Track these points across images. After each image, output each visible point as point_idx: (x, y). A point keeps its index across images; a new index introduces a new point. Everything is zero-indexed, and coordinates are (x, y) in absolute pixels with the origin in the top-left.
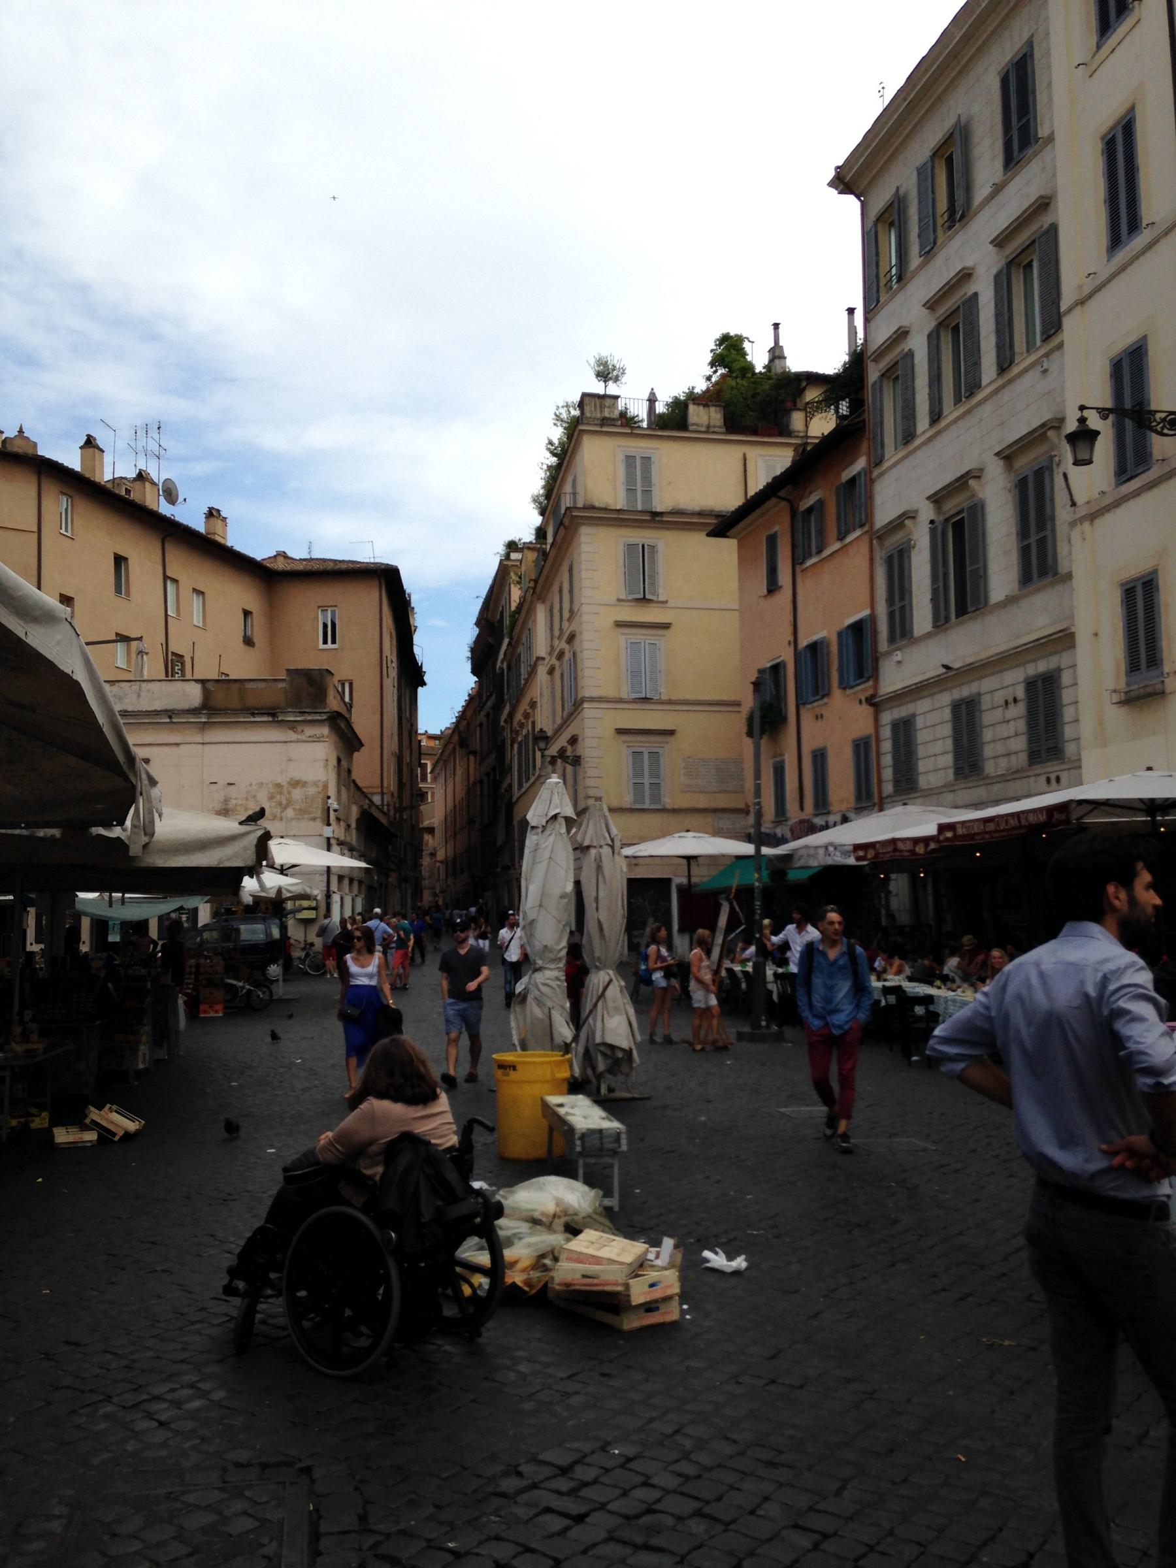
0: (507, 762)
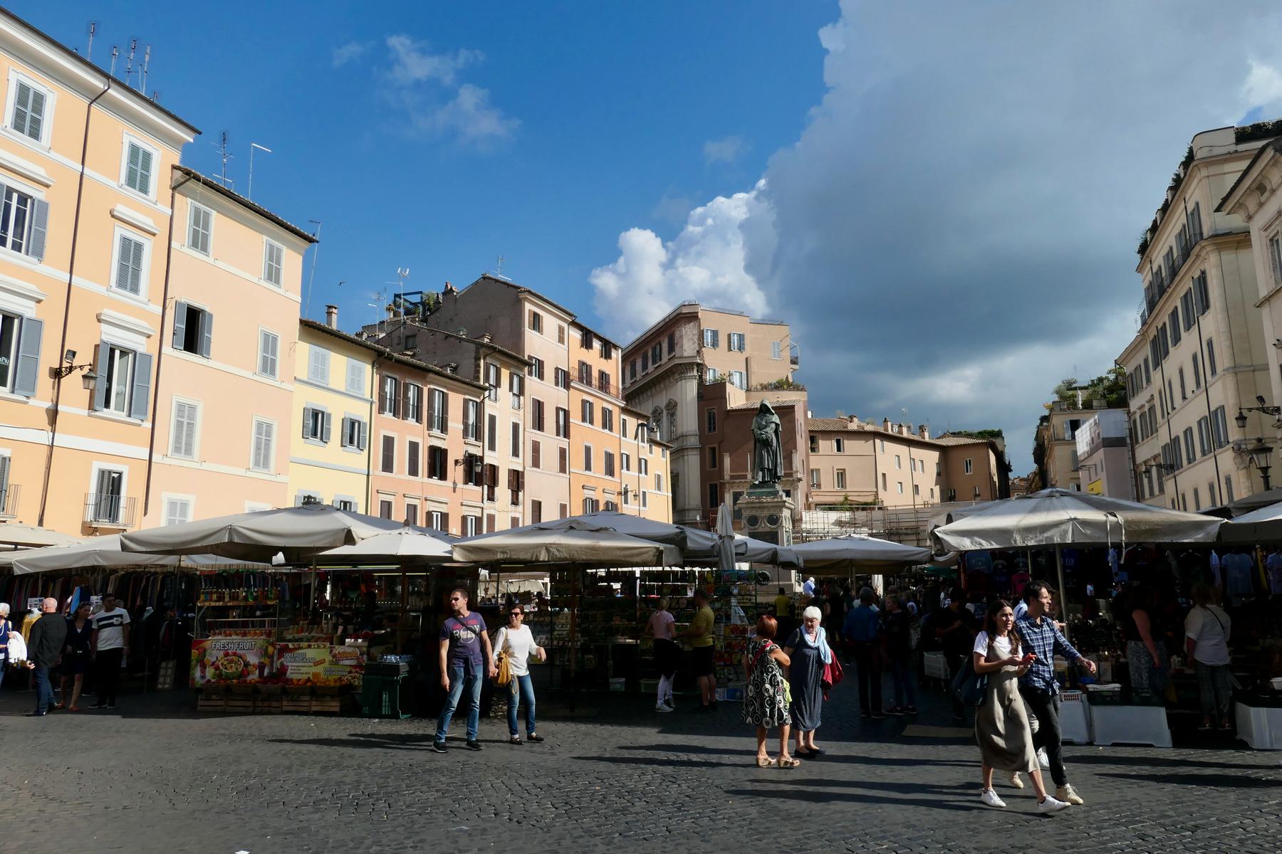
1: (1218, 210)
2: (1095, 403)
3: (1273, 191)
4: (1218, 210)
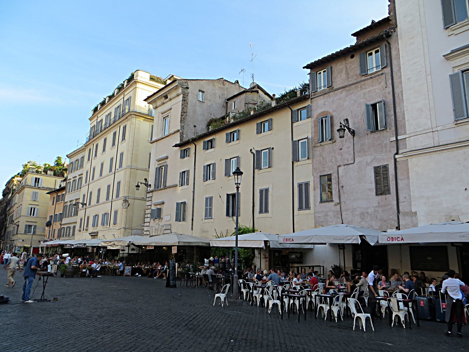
0: (7, 219)
1: (145, 100)
2: (49, 172)
3: (171, 100)
4: (145, 100)
